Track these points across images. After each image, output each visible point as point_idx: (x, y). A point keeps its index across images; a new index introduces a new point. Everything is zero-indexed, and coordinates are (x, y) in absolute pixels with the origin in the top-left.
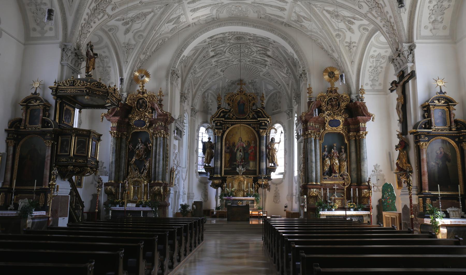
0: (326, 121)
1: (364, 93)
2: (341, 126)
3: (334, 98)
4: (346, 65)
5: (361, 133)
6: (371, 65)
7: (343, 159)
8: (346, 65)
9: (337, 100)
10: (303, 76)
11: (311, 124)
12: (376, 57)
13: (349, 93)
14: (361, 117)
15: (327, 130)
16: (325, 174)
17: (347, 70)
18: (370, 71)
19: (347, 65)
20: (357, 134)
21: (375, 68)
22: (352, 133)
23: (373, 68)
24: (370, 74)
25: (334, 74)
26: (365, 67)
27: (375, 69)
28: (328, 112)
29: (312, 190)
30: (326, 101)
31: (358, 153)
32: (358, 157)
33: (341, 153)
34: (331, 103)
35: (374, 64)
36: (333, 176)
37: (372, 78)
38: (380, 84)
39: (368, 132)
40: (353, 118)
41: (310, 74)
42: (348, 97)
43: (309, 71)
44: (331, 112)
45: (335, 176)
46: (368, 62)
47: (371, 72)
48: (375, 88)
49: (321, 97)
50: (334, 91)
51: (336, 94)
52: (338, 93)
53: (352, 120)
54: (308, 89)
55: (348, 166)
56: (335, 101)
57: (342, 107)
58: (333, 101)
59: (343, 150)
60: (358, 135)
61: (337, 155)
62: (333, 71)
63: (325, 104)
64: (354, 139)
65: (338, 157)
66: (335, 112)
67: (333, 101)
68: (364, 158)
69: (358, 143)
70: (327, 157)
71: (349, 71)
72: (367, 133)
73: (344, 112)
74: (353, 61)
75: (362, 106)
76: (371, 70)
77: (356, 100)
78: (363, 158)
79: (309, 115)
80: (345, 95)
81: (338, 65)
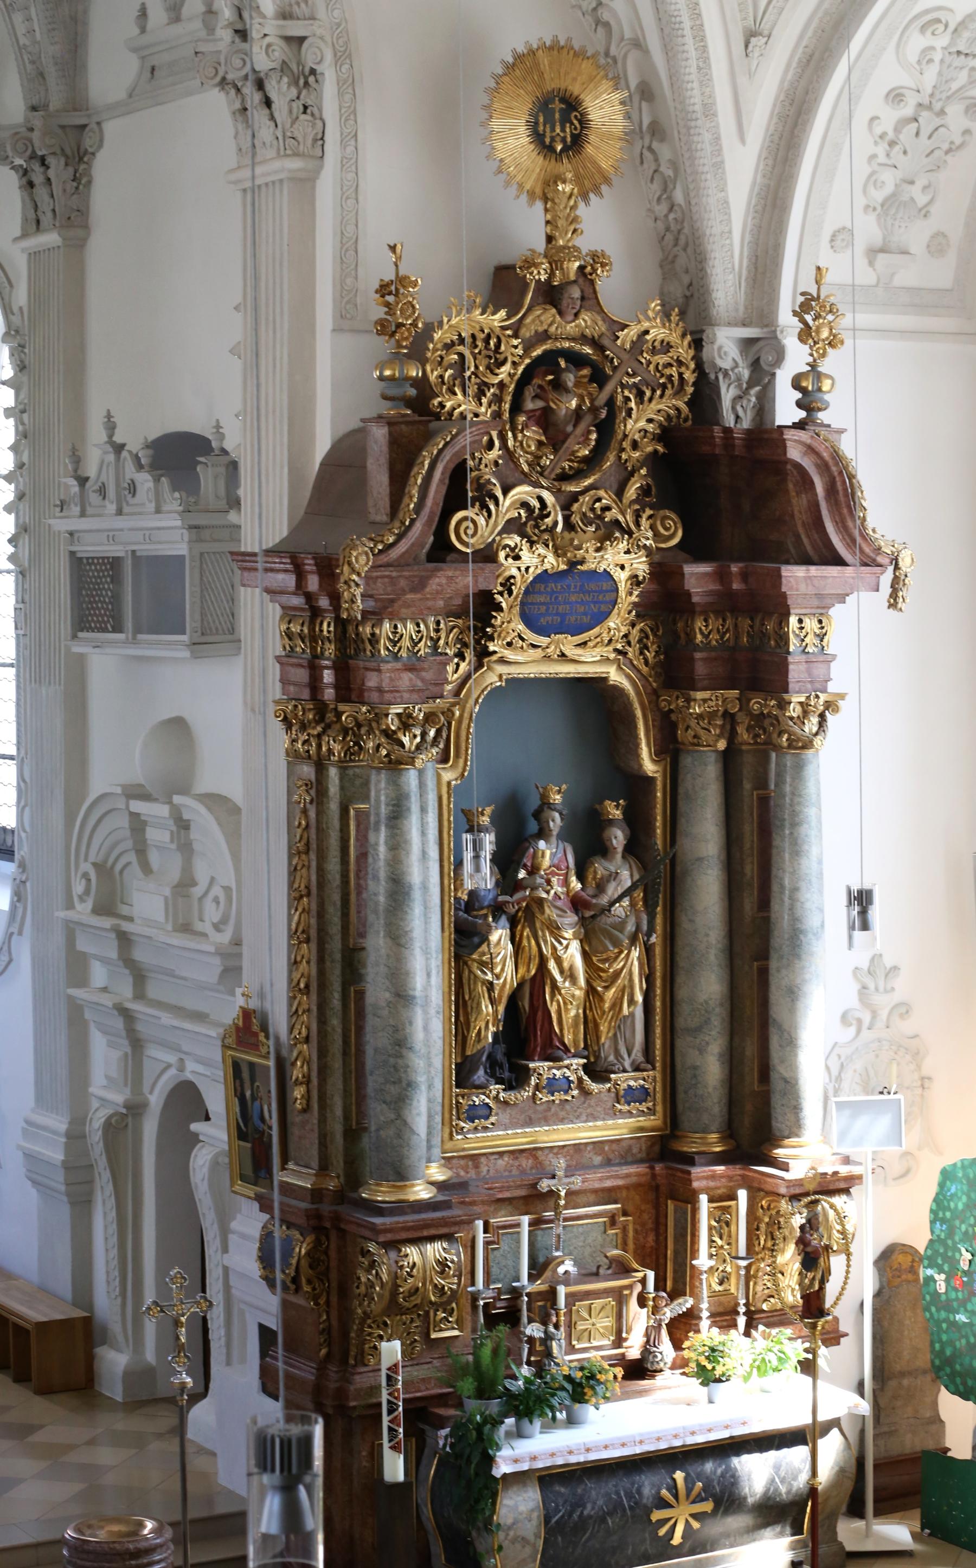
0: (508, 585)
1: (833, 342)
2: (616, 623)
3: (576, 360)
4: (693, 54)
5: (794, 710)
6: (903, 79)
7: (621, 926)
8: (693, 54)
9: (599, 378)
10: (280, 90)
11: (406, 643)
12: (962, 24)
13: (677, 291)
14: (813, 569)
15: (502, 661)
16: (480, 1075)
17: (695, 98)
18: (887, 125)
19: (703, 50)
20: (743, 702)
21: (929, 107)
22: (706, 694)
23: (909, 111)
24: (881, 150)
25: (584, 122)
26: (850, 95)
27: (925, 115)
28: (522, 491)
29: (413, 1253)
30: (501, 385)
31: (750, 869)
32: (749, 905)
33: (600, 868)
34: (540, 404)
35: (930, 77)
36: (537, 1087)
37: (889, 189)
38: (937, 244)
39: (842, 696)
40: (734, 568)
41: (348, 85)
42: (684, 351)
43: (344, 56)
44: (540, 499)
45: (552, 1086)
46: (889, 54)
47: (891, 135)
48: (897, 281)
49: (462, 341)
50: (576, 293)
51: (586, 321)
52: (601, 311)
53: (722, 576)
54: (384, 289)
55: (658, 983)
56: (577, 384)
57: (635, 446)
58: (558, 385)
59: (618, 838)
60: (750, 713)
61: (566, 883)
62: (575, 89)
63: (497, 415)
64: (722, 745)
65: (577, 903)
66: (575, 497)
67: (558, 385)
68: (801, 932)
69: (747, 786)
70: (498, 910)
71: (709, 111)
72: (836, 710)
73: (645, 491)
74: (765, 27)
75: (823, 467)
76: (889, 117)
77: (746, 374)
78: (796, 936)
79: (398, 564)
80: (657, 333)
81: (605, 16)
